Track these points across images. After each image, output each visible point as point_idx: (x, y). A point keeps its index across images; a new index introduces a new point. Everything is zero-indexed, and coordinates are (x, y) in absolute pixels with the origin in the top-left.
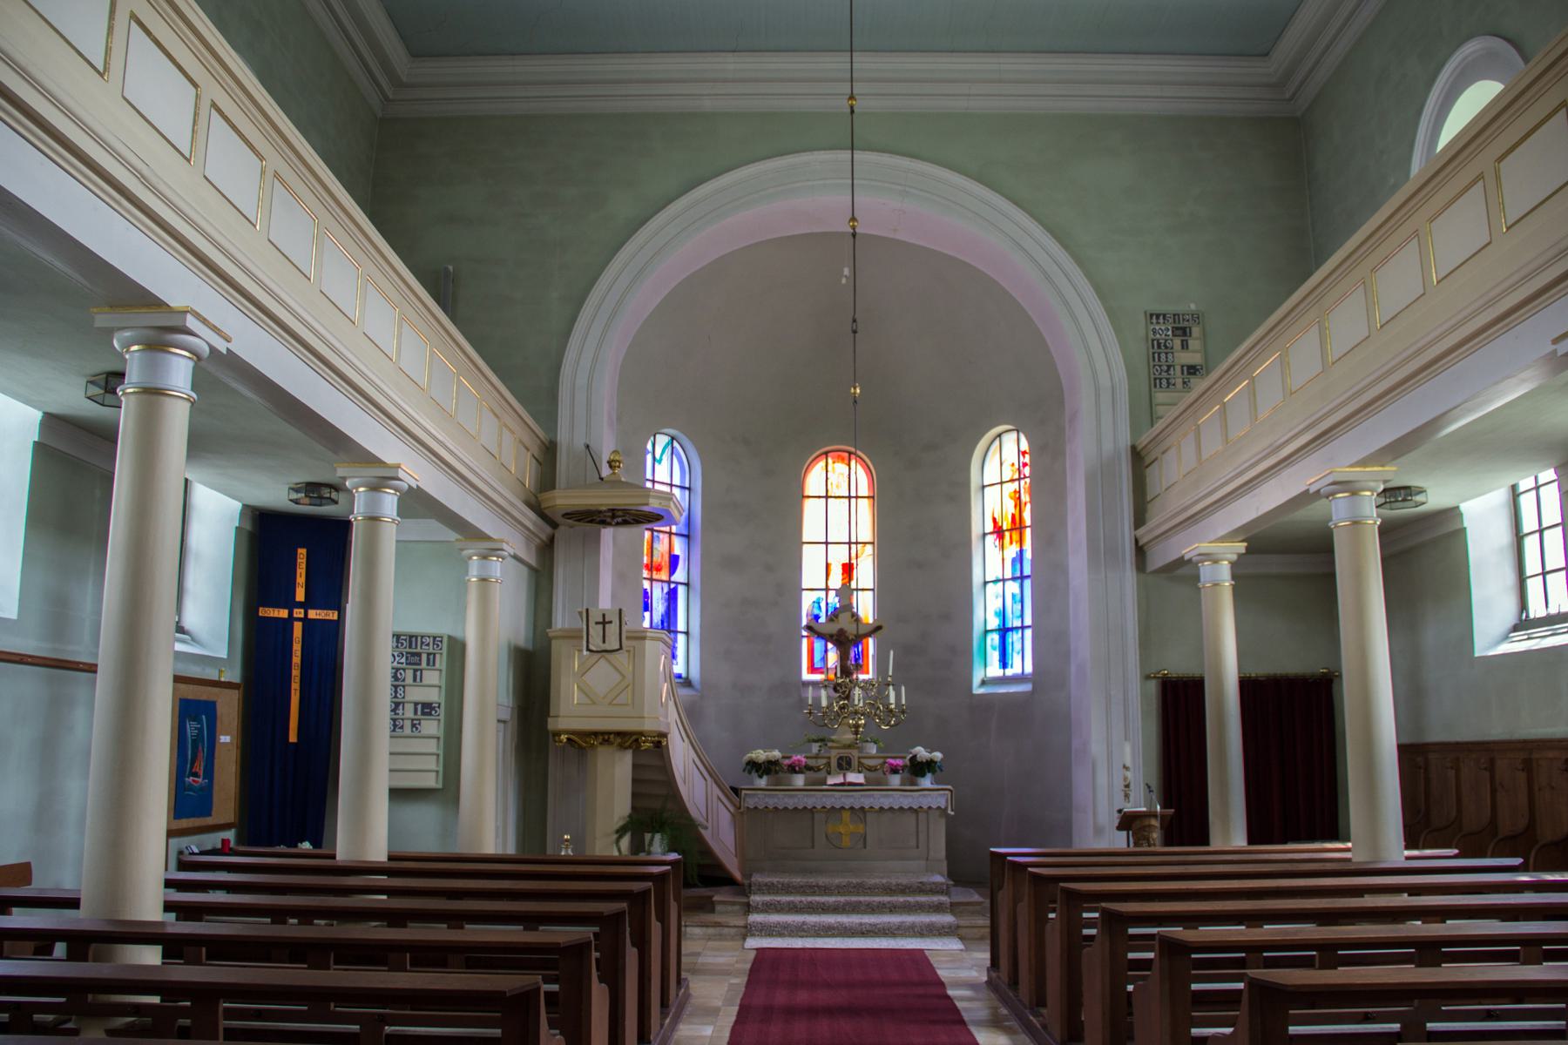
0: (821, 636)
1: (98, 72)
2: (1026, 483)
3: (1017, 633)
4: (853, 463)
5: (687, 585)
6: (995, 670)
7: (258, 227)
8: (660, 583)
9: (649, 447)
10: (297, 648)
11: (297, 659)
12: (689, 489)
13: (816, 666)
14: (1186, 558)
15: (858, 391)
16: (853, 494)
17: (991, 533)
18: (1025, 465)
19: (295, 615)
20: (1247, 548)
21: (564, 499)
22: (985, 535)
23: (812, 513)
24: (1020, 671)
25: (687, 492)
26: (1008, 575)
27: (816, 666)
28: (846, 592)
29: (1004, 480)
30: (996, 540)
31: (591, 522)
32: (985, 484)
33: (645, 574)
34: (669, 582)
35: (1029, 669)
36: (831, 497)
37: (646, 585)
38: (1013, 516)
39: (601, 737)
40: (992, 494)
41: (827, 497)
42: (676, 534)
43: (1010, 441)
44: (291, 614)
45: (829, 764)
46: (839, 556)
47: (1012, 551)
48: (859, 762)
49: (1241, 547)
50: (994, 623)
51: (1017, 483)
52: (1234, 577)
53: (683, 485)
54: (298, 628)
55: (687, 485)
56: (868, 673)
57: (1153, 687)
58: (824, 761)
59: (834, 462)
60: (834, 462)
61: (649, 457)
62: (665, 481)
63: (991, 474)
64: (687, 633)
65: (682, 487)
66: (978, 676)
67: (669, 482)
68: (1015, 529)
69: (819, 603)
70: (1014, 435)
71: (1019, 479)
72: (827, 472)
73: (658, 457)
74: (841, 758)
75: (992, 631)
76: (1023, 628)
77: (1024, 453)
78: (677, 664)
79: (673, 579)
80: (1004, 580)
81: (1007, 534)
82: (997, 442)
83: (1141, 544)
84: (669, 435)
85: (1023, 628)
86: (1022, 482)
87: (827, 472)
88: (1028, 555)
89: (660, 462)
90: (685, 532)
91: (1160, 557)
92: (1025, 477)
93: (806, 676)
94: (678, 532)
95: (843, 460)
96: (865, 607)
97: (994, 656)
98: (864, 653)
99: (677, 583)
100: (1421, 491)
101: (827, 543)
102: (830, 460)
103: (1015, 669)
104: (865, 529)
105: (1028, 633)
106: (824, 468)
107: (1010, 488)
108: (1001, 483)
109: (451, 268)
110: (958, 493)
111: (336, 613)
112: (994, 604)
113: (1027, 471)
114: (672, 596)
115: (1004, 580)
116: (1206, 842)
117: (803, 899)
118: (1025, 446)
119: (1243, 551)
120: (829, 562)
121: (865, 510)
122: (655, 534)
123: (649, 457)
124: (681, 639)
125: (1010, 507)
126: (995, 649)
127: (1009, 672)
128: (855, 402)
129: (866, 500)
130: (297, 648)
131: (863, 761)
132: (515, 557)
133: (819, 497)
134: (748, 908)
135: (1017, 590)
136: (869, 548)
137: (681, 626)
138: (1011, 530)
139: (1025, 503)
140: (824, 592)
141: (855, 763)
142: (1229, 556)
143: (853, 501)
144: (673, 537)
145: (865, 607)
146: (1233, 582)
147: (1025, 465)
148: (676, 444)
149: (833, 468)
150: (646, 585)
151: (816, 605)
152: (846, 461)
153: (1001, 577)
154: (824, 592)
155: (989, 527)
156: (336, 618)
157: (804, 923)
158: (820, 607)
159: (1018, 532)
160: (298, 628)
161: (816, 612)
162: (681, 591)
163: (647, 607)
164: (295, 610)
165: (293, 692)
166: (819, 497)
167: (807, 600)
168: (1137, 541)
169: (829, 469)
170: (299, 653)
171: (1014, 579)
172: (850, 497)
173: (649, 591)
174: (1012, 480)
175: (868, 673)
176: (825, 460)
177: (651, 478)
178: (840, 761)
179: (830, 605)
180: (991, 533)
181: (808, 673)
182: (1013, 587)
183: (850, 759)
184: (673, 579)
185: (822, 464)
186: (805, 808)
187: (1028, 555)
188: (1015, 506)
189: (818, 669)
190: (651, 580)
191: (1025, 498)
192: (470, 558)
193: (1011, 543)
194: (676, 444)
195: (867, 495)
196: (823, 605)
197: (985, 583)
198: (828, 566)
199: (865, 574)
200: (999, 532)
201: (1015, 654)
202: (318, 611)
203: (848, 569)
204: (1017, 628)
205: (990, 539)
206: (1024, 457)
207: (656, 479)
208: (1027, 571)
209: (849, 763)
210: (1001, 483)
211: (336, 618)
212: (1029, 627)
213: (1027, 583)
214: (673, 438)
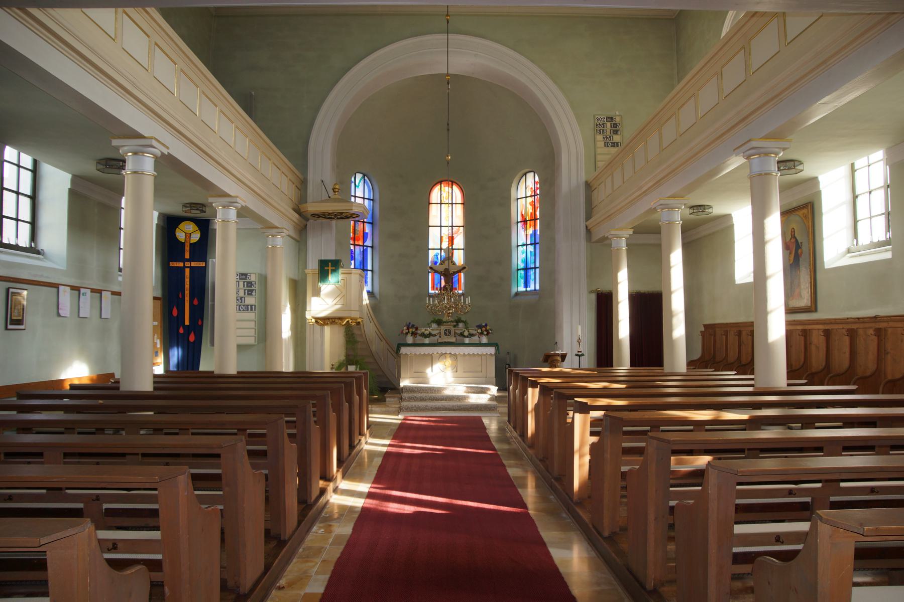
0: (436, 272)
1: (112, 39)
2: (537, 197)
3: (532, 271)
4: (454, 187)
5: (372, 247)
6: (521, 288)
7: (175, 95)
9: (353, 179)
10: (187, 280)
11: (187, 286)
12: (373, 200)
14: (606, 236)
15: (450, 158)
16: (454, 202)
17: (521, 222)
18: (537, 189)
19: (186, 265)
20: (633, 232)
21: (312, 207)
22: (518, 222)
23: (434, 210)
24: (534, 289)
25: (372, 202)
26: (529, 242)
28: (450, 251)
29: (527, 196)
30: (523, 225)
31: (325, 218)
32: (518, 197)
33: (352, 242)
34: (363, 246)
35: (538, 288)
37: (352, 247)
38: (531, 213)
39: (331, 320)
40: (521, 202)
41: (441, 204)
42: (366, 222)
43: (530, 176)
44: (188, 267)
45: (440, 333)
46: (446, 232)
47: (530, 231)
48: (455, 332)
49: (631, 232)
50: (521, 266)
51: (533, 197)
52: (627, 245)
54: (187, 271)
55: (372, 198)
57: (593, 297)
58: (438, 331)
59: (444, 186)
60: (444, 186)
61: (353, 185)
63: (521, 193)
64: (372, 271)
65: (369, 199)
66: (514, 290)
68: (532, 220)
69: (437, 256)
70: (532, 174)
71: (534, 196)
72: (441, 191)
73: (357, 184)
74: (446, 330)
75: (521, 269)
76: (535, 268)
77: (537, 183)
79: (365, 244)
80: (527, 245)
81: (528, 222)
82: (524, 177)
83: (588, 228)
84: (362, 174)
85: (535, 268)
86: (536, 197)
87: (441, 191)
88: (538, 233)
91: (597, 235)
92: (537, 195)
93: (431, 291)
96: (459, 258)
97: (522, 282)
98: (459, 281)
99: (367, 246)
100: (710, 207)
101: (441, 226)
102: (442, 185)
103: (531, 287)
104: (459, 220)
105: (537, 270)
107: (530, 200)
108: (526, 197)
109: (253, 93)
110: (505, 201)
111: (204, 263)
112: (522, 256)
113: (538, 192)
114: (364, 253)
115: (527, 245)
116: (612, 367)
117: (427, 395)
118: (537, 179)
119: (632, 233)
120: (442, 235)
121: (459, 211)
123: (353, 185)
124: (369, 273)
125: (530, 209)
126: (522, 278)
127: (528, 289)
128: (448, 163)
129: (460, 205)
130: (187, 280)
131: (456, 331)
132: (289, 236)
133: (437, 204)
134: (401, 399)
135: (533, 250)
136: (462, 229)
137: (369, 267)
138: (530, 220)
139: (537, 208)
140: (440, 250)
141: (453, 333)
142: (625, 235)
143: (454, 205)
144: (365, 224)
145: (459, 258)
146: (627, 248)
147: (537, 189)
148: (366, 178)
149: (444, 189)
153: (525, 243)
154: (440, 250)
155: (520, 219)
156: (204, 265)
157: (426, 406)
158: (437, 258)
159: (534, 221)
160: (187, 271)
161: (436, 260)
162: (369, 250)
163: (353, 258)
164: (186, 263)
165: (186, 301)
166: (437, 204)
167: (431, 254)
168: (586, 227)
170: (188, 283)
171: (531, 244)
172: (452, 204)
173: (353, 250)
174: (531, 196)
176: (440, 186)
177: (354, 195)
179: (442, 257)
180: (521, 222)
182: (531, 248)
184: (365, 244)
185: (439, 187)
186: (429, 354)
187: (538, 233)
188: (532, 209)
190: (354, 245)
191: (537, 205)
192: (268, 236)
193: (530, 227)
194: (366, 178)
195: (460, 202)
196: (439, 257)
197: (518, 246)
198: (441, 237)
199: (459, 242)
200: (525, 221)
201: (531, 281)
202: (196, 263)
203: (451, 239)
204: (532, 268)
205: (520, 225)
206: (537, 185)
208: (538, 241)
209: (450, 333)
210: (526, 197)
211: (204, 265)
212: (538, 268)
213: (538, 246)
214: (364, 175)
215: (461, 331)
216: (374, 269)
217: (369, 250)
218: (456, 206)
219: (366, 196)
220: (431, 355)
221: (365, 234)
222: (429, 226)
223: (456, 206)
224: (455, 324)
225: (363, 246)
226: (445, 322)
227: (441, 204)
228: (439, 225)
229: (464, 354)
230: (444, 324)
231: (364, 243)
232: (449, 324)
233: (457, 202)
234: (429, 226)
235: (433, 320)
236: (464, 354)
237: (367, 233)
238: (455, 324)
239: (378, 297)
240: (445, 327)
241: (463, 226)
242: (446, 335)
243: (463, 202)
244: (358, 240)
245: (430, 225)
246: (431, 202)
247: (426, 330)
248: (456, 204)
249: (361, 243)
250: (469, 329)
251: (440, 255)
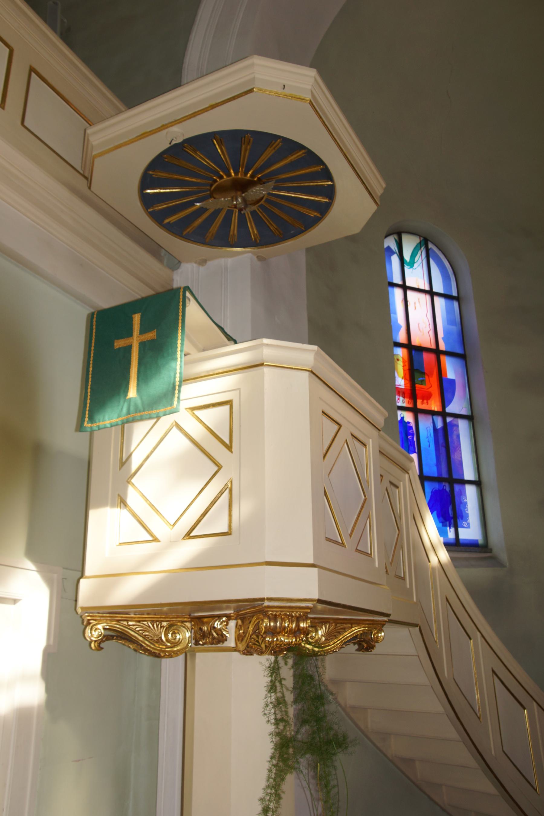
5: (470, 418)
8: (430, 417)
12: (457, 299)
33: (401, 402)
37: (408, 417)
53: (447, 293)
55: (455, 294)
61: (395, 259)
62: (422, 287)
64: (478, 483)
67: (427, 288)
73: (407, 256)
78: (468, 527)
79: (448, 410)
84: (420, 236)
89: (412, 264)
90: (459, 350)
94: (449, 350)
122: (449, 420)
137: (469, 474)
150: (408, 417)
162: (463, 426)
173: (413, 424)
184: (448, 410)
190: (415, 411)
194: (430, 246)
207: (408, 284)
216: (485, 479)
217: (463, 426)
219: (438, 287)
221: (445, 385)
225: (443, 414)
231: (444, 406)
237: (453, 382)
239: (504, 557)
244: (427, 397)
249: (435, 406)
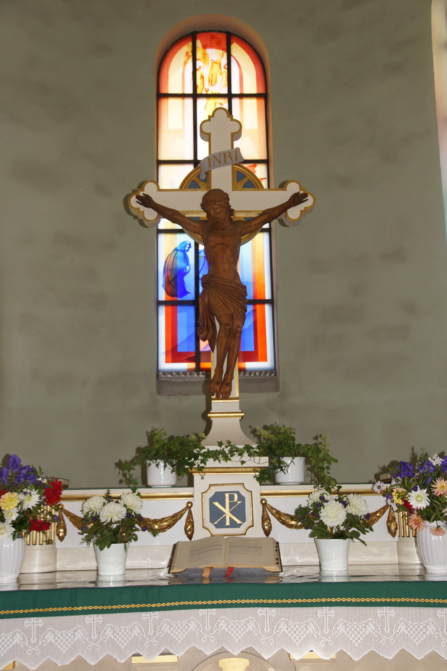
4: (236, 49)
13: (180, 349)
16: (235, 90)
27: (180, 349)
36: (202, 96)
41: (195, 96)
48: (264, 505)
56: (265, 359)
59: (205, 47)
60: (205, 47)
69: (184, 252)
95: (217, 46)
102: (199, 44)
106: (190, 54)
131: (271, 501)
133: (183, 96)
149: (205, 55)
151: (180, 254)
152: (225, 47)
158: (186, 258)
161: (180, 264)
166: (183, 96)
169: (199, 55)
175: (265, 359)
176: (190, 44)
178: (217, 504)
181: (167, 362)
183: (241, 498)
185: (187, 48)
189: (182, 354)
195: (254, 91)
215: (304, 501)
218: (241, 105)
220: (129, 663)
222: (161, 163)
223: (241, 105)
224: (264, 461)
226: (215, 455)
227: (195, 96)
228: (191, 158)
229: (341, 654)
230: (211, 463)
232: (235, 461)
233: (245, 92)
234: (161, 163)
235: (144, 443)
236: (341, 654)
238: (264, 461)
240: (210, 478)
241: (266, 162)
242: (221, 525)
243: (262, 91)
245: (162, 157)
246: (163, 91)
247: (109, 498)
248: (241, 96)
250: (345, 488)
251: (192, 250)
